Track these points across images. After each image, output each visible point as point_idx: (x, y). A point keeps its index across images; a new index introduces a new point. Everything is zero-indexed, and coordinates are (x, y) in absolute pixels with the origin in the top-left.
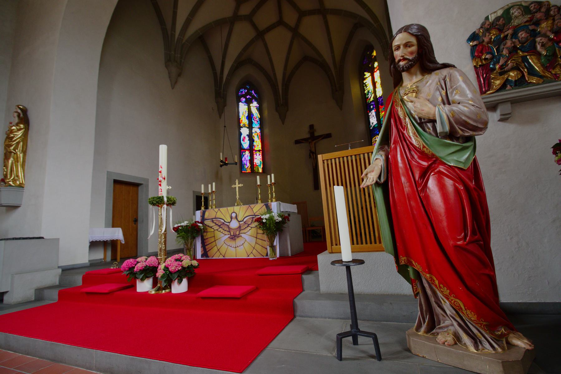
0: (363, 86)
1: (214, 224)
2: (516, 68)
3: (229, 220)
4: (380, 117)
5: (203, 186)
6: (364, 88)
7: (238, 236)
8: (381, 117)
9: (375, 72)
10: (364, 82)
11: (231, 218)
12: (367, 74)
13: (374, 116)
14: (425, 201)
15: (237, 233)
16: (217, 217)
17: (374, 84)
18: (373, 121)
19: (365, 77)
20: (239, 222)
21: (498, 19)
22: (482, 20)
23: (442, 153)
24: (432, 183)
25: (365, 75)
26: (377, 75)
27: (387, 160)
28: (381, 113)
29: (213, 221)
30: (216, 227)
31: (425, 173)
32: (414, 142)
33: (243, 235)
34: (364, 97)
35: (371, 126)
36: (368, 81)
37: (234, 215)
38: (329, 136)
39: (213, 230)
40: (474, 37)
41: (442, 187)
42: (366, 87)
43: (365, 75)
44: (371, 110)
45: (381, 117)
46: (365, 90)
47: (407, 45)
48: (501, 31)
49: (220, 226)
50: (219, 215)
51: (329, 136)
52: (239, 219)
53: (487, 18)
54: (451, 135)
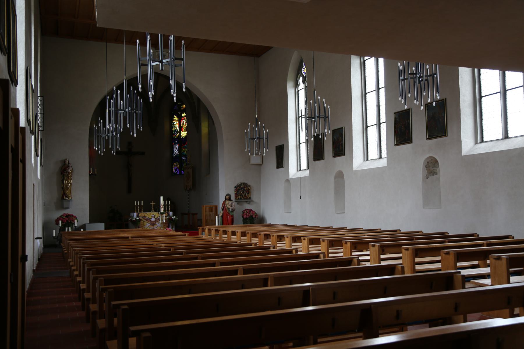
0: (172, 125)
1: (143, 219)
2: (240, 196)
3: (151, 218)
4: (181, 151)
5: (136, 202)
6: (172, 126)
7: (155, 224)
8: (182, 152)
9: (182, 120)
10: (173, 122)
11: (152, 217)
12: (176, 118)
13: (177, 148)
14: (227, 219)
15: (155, 223)
16: (145, 216)
17: (180, 127)
18: (176, 151)
19: (174, 118)
20: (155, 218)
21: (240, 185)
22: (237, 184)
23: (230, 213)
24: (229, 217)
25: (174, 117)
26: (184, 122)
27: (223, 212)
28: (182, 149)
29: (143, 218)
30: (145, 220)
31: (228, 215)
32: (227, 211)
33: (157, 224)
34: (172, 133)
35: (174, 155)
36: (176, 123)
37: (153, 216)
38: (143, 153)
39: (143, 221)
40: (235, 187)
41: (229, 217)
42: (174, 126)
43: (174, 117)
44: (175, 144)
45: (182, 152)
46: (172, 128)
47: (228, 197)
48: (240, 187)
49: (146, 220)
50: (146, 215)
51: (143, 153)
52: (156, 218)
53: (238, 184)
54: (232, 211)
